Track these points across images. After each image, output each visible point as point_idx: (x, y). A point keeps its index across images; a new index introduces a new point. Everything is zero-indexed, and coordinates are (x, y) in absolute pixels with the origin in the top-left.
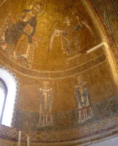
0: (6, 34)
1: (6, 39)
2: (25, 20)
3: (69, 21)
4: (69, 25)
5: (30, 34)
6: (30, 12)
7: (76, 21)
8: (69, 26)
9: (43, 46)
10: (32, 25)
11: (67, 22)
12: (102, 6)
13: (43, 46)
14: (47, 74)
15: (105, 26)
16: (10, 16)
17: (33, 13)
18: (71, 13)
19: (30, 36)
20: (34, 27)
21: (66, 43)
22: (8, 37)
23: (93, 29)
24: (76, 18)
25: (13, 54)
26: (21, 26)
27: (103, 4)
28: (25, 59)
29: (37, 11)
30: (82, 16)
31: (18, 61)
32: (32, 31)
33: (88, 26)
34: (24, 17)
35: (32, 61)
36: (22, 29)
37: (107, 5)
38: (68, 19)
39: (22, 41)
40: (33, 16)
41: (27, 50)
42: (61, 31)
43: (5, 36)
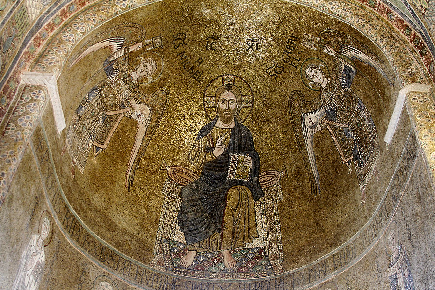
0: (182, 225)
2: (218, 152)
3: (319, 74)
4: (325, 83)
5: (251, 176)
6: (217, 125)
7: (331, 61)
8: (329, 85)
9: (295, 183)
10: (241, 149)
11: (316, 80)
13: (295, 183)
14: (324, 264)
15: (402, 22)
16: (174, 173)
17: (226, 121)
18: (307, 51)
19: (251, 181)
20: (251, 150)
21: (347, 135)
22: (192, 225)
23: (376, 56)
24: (325, 54)
25: (221, 261)
26: (216, 173)
28: (259, 252)
29: (232, 107)
31: (239, 271)
32: (250, 165)
33: (362, 56)
34: (210, 149)
35: (280, 247)
36: (222, 179)
38: (313, 71)
39: (235, 210)
40: (232, 125)
41: (259, 224)
42: (318, 113)
43: (181, 230)
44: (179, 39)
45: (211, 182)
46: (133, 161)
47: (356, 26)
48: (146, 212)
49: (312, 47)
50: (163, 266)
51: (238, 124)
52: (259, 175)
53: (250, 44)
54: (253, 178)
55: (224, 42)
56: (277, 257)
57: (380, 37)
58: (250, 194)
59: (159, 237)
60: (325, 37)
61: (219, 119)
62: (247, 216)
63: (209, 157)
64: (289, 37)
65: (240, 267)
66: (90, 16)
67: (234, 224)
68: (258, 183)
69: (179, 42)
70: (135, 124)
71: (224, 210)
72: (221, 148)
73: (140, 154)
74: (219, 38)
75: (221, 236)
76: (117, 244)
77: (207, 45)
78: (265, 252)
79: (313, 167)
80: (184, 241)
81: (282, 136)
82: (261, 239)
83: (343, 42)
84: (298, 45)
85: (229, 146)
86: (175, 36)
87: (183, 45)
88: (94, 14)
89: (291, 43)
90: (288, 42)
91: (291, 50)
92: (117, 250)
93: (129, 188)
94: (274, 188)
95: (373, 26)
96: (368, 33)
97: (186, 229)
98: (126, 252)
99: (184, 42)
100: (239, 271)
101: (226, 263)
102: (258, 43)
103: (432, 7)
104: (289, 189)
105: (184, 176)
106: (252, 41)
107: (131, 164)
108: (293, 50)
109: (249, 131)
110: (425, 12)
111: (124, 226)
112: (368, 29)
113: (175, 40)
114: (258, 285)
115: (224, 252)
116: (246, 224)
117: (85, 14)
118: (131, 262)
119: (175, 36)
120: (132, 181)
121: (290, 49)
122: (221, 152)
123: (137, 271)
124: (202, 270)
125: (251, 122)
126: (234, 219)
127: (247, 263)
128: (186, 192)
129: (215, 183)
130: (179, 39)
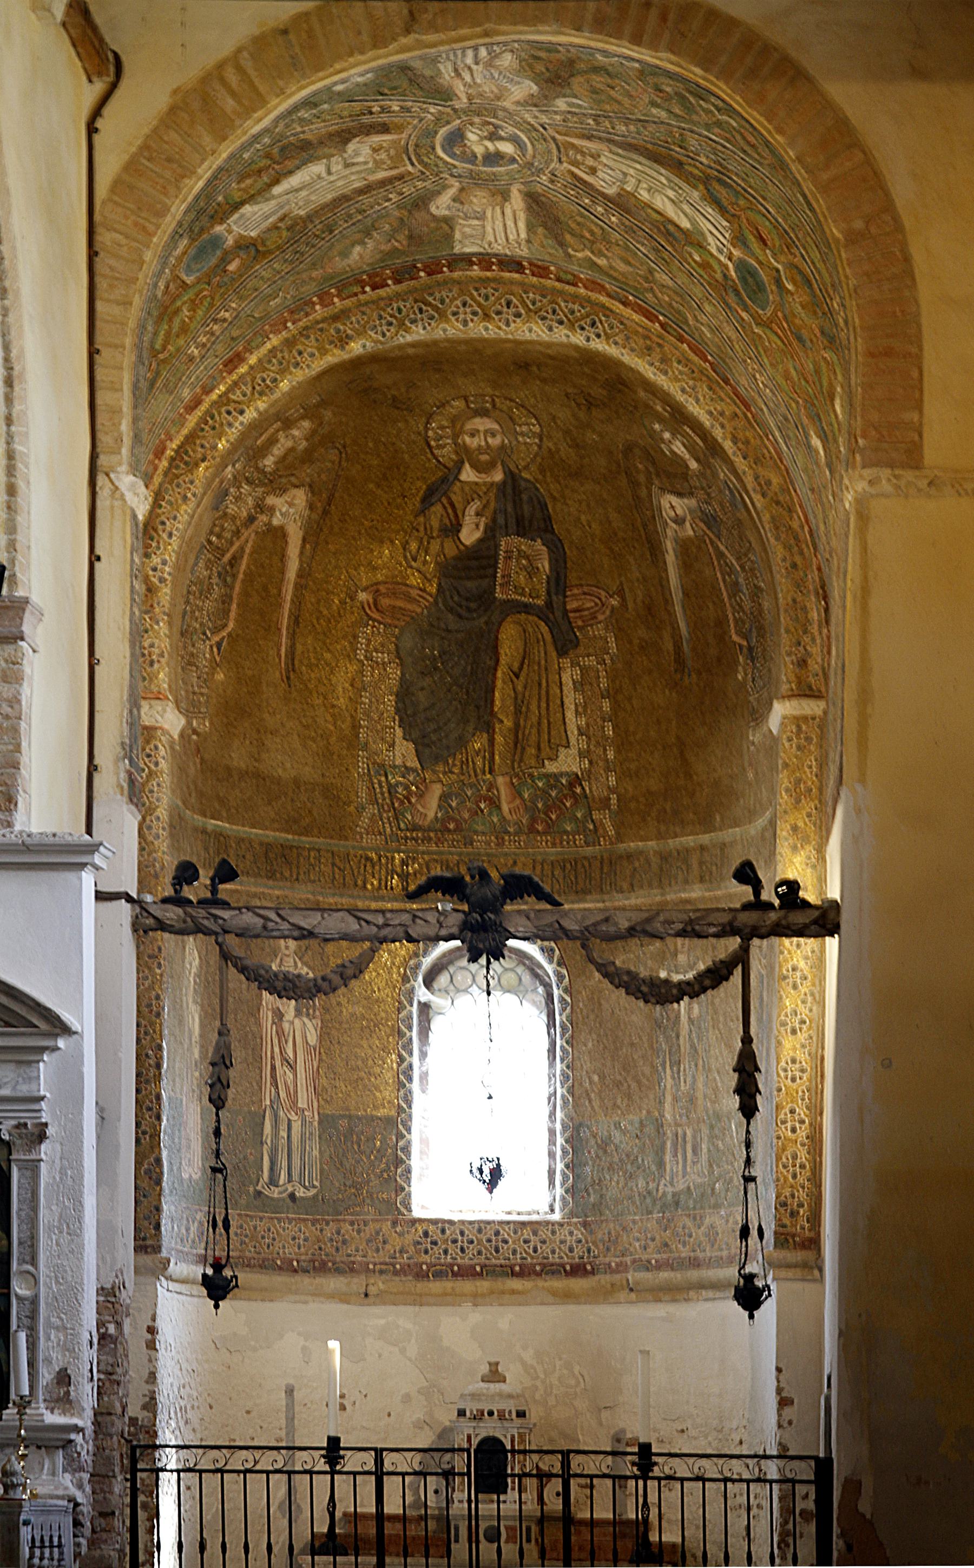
1: (423, 746)
2: (470, 535)
5: (548, 593)
6: (463, 477)
9: (642, 632)
10: (522, 529)
19: (549, 604)
20: (546, 531)
25: (494, 804)
26: (469, 584)
28: (571, 785)
31: (532, 830)
34: (454, 529)
35: (612, 781)
36: (485, 599)
40: (498, 476)
41: (570, 715)
45: (461, 606)
46: (286, 616)
48: (329, 718)
50: (380, 834)
51: (511, 472)
52: (565, 592)
54: (554, 597)
56: (605, 803)
58: (548, 637)
59: (362, 766)
61: (467, 465)
62: (543, 692)
63: (451, 550)
65: (533, 820)
67: (518, 712)
68: (566, 612)
70: (279, 534)
71: (494, 675)
72: (477, 526)
73: (298, 587)
75: (492, 742)
76: (290, 824)
78: (581, 785)
79: (678, 608)
80: (413, 763)
81: (613, 515)
82: (573, 751)
85: (494, 520)
92: (290, 837)
93: (288, 678)
94: (598, 630)
97: (416, 734)
98: (306, 832)
100: (532, 830)
101: (505, 808)
104: (630, 642)
105: (400, 603)
107: (285, 621)
109: (537, 489)
111: (293, 773)
114: (568, 866)
115: (500, 780)
116: (544, 712)
118: (319, 851)
120: (293, 660)
122: (478, 535)
123: (333, 864)
124: (458, 829)
125: (542, 471)
126: (516, 698)
127: (548, 809)
128: (408, 642)
129: (469, 610)
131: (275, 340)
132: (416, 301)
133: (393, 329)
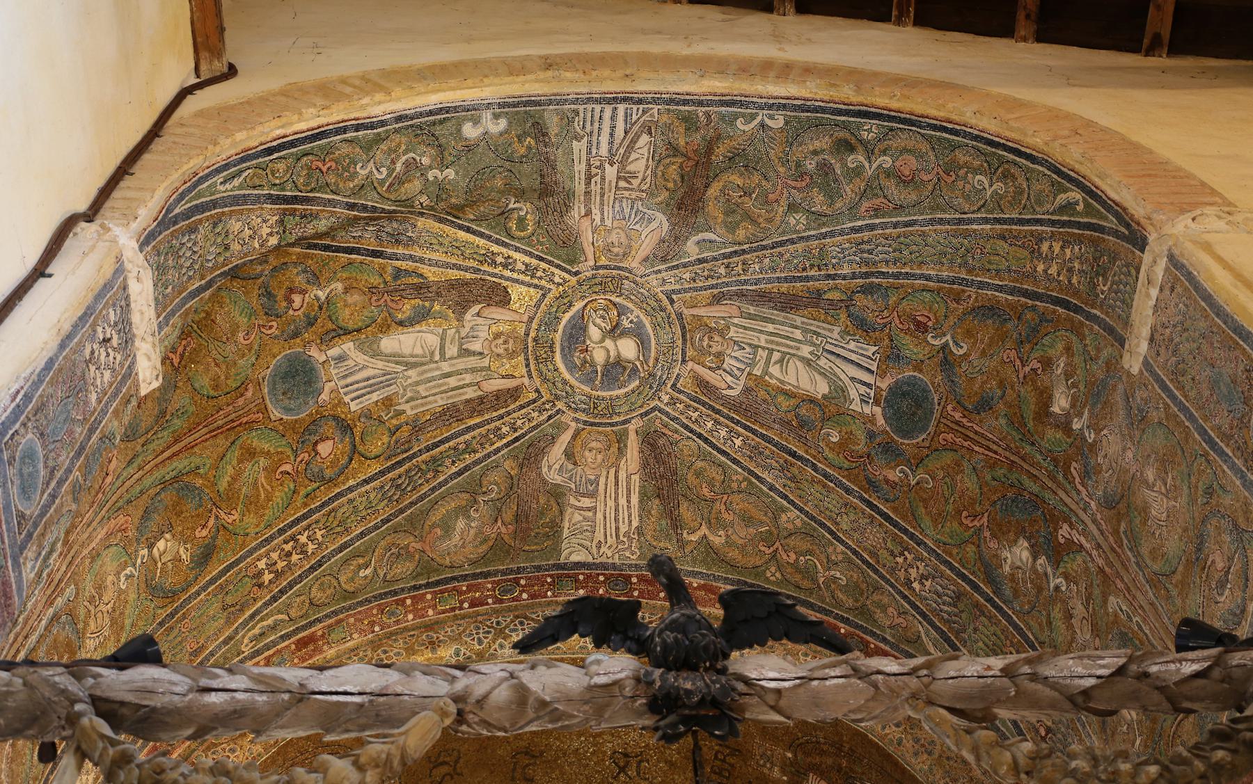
12: (884, 609)
27: (877, 588)
30: (830, 761)
37: (902, 574)
44: (445, 763)
47: (882, 738)
49: (776, 773)
53: (622, 764)
55: (555, 761)
57: (944, 778)
60: (807, 754)
64: (716, 748)
66: (222, 754)
69: (444, 770)
74: (541, 753)
77: (514, 770)
83: (851, 770)
84: (741, 767)
86: (433, 759)
87: (452, 778)
88: (231, 746)
89: (724, 761)
90: (716, 757)
91: (724, 776)
95: (922, 741)
96: (913, 760)
99: (455, 769)
102: (641, 761)
103: (1063, 729)
106: (626, 755)
108: (728, 778)
110: (1046, 735)
112: (911, 750)
113: (434, 767)
117: (208, 748)
119: (433, 759)
121: (720, 774)
130: (445, 763)
131: (357, 639)
132: (517, 617)
133: (490, 636)
